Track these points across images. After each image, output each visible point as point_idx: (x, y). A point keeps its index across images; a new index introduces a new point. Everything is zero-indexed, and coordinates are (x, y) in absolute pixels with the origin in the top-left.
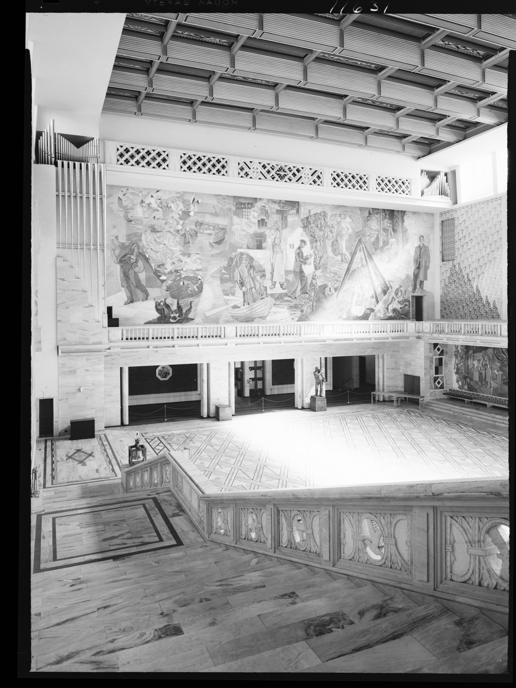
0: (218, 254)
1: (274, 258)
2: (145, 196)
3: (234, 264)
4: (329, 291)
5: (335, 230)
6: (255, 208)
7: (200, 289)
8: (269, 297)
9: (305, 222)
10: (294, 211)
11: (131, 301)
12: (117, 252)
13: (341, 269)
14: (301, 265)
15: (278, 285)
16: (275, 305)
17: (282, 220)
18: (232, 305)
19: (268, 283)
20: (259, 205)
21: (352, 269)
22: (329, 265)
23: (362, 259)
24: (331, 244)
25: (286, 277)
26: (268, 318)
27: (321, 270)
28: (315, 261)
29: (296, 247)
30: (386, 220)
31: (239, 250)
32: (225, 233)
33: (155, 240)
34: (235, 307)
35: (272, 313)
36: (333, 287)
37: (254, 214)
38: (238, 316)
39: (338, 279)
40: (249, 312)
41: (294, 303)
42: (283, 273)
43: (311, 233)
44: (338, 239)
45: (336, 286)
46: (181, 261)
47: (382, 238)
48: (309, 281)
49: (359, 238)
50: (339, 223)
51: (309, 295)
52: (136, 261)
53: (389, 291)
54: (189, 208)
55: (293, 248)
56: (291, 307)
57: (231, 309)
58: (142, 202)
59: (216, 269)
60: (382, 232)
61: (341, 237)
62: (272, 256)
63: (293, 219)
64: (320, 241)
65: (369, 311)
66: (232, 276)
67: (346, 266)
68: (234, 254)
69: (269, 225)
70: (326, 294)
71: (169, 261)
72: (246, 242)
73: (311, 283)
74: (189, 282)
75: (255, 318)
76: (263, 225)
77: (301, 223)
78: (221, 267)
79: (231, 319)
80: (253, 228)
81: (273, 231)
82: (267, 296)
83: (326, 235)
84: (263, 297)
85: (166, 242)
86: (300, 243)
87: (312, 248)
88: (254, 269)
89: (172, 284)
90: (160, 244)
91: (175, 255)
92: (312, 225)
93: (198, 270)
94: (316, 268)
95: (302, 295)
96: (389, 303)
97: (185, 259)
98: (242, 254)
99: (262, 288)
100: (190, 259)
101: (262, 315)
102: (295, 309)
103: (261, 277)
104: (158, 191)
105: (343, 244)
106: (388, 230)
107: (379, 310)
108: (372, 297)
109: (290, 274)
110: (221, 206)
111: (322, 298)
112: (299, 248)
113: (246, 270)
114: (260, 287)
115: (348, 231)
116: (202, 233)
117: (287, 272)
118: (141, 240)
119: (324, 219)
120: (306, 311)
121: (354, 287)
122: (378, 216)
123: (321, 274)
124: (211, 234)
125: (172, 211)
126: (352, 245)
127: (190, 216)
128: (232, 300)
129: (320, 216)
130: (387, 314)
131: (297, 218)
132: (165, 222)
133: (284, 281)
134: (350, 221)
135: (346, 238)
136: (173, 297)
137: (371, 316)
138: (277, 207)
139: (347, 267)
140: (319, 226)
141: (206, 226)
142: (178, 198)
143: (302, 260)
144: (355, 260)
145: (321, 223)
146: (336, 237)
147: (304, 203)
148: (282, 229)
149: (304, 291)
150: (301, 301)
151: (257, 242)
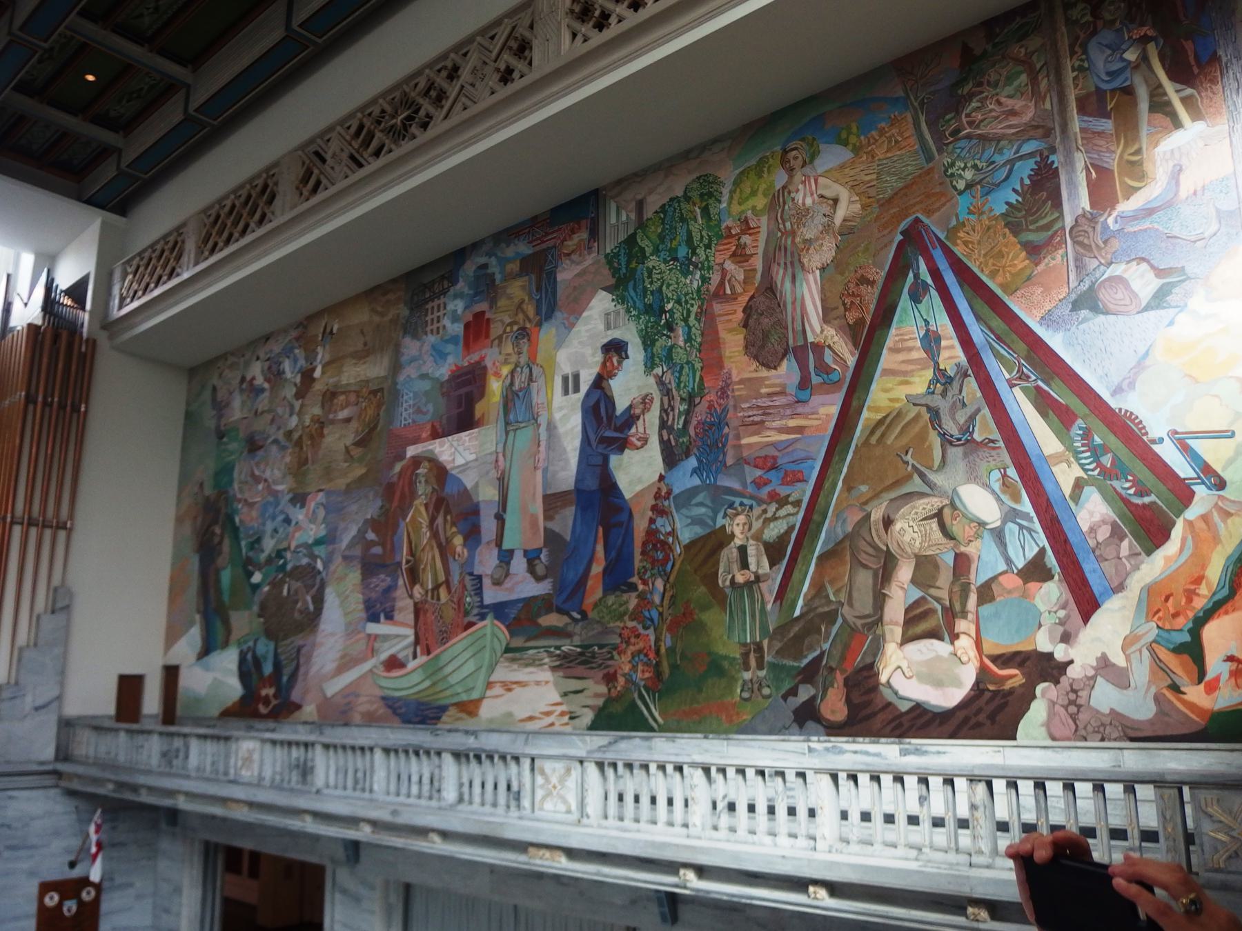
0: (361, 479)
1: (508, 454)
2: (247, 364)
3: (395, 503)
4: (735, 567)
5: (757, 245)
6: (461, 286)
7: (319, 601)
8: (487, 622)
9: (623, 260)
10: (584, 235)
11: (207, 649)
12: (200, 519)
13: (800, 430)
14: (606, 460)
15: (519, 564)
16: (508, 650)
17: (539, 289)
18: (384, 656)
19: (487, 562)
20: (469, 268)
21: (867, 416)
22: (734, 423)
23: (931, 341)
24: (740, 315)
25: (550, 525)
26: (487, 710)
27: (692, 462)
28: (663, 425)
29: (587, 378)
30: (1107, 36)
31: (411, 451)
32: (379, 406)
33: (253, 475)
34: (393, 663)
35: (497, 690)
36: (758, 537)
37: (454, 311)
38: (399, 699)
39: (783, 491)
40: (427, 683)
41: (577, 640)
42: (538, 508)
43: (649, 299)
44: (779, 274)
45: (773, 532)
46: (287, 521)
47: (1080, 160)
48: (640, 526)
49: (903, 225)
50: (778, 200)
51: (642, 597)
52: (220, 543)
53: (1192, 513)
54: (315, 359)
55: (577, 390)
56: (567, 665)
57: (380, 671)
58: (243, 379)
59: (353, 531)
60: (1076, 123)
61: (796, 266)
62: (500, 449)
63: (580, 268)
64: (686, 320)
65: (1014, 677)
66: (389, 547)
67: (828, 408)
68: (398, 467)
69: (496, 330)
70: (723, 581)
71: (269, 526)
72: (428, 417)
73: (651, 533)
74: (299, 584)
75: (443, 709)
76: (477, 337)
77: (606, 271)
78: (366, 521)
79: (382, 711)
80: (450, 359)
81: (509, 348)
82: (483, 617)
83: (715, 278)
84: (471, 618)
85: (268, 474)
86: (599, 357)
87: (650, 365)
88: (447, 512)
89: (269, 593)
90: (257, 480)
91: (280, 508)
92: (653, 261)
93: (318, 542)
94: (671, 457)
95: (611, 600)
96: (1200, 603)
97: (299, 515)
98: (416, 461)
99: (468, 578)
100: (304, 511)
101: (464, 697)
102: (580, 670)
103: (466, 539)
104: (268, 339)
105: (807, 295)
106: (1129, 91)
107: (1104, 664)
108: (1035, 571)
109: (564, 506)
110: (377, 319)
111: (705, 608)
112: (600, 383)
113: (424, 520)
114: (462, 581)
115: (831, 217)
116: (332, 422)
117: (553, 502)
118: (231, 482)
119: (706, 211)
120: (629, 680)
121: (888, 522)
122: (1035, 42)
123: (696, 481)
124: (348, 420)
125: (286, 380)
126: (864, 281)
127: (314, 380)
128: (386, 638)
129: (685, 206)
130: (1195, 694)
131: (589, 260)
132: (269, 417)
133: (539, 542)
134: (845, 154)
135: (825, 253)
136: (270, 634)
137: (1037, 712)
138: (524, 248)
139: (835, 410)
140: (683, 252)
141: (342, 398)
142: (297, 339)
143: (609, 434)
144: (887, 360)
145: (689, 240)
146: (767, 271)
147: (619, 182)
148: (539, 324)
149: (617, 578)
150: (607, 631)
151: (459, 406)
